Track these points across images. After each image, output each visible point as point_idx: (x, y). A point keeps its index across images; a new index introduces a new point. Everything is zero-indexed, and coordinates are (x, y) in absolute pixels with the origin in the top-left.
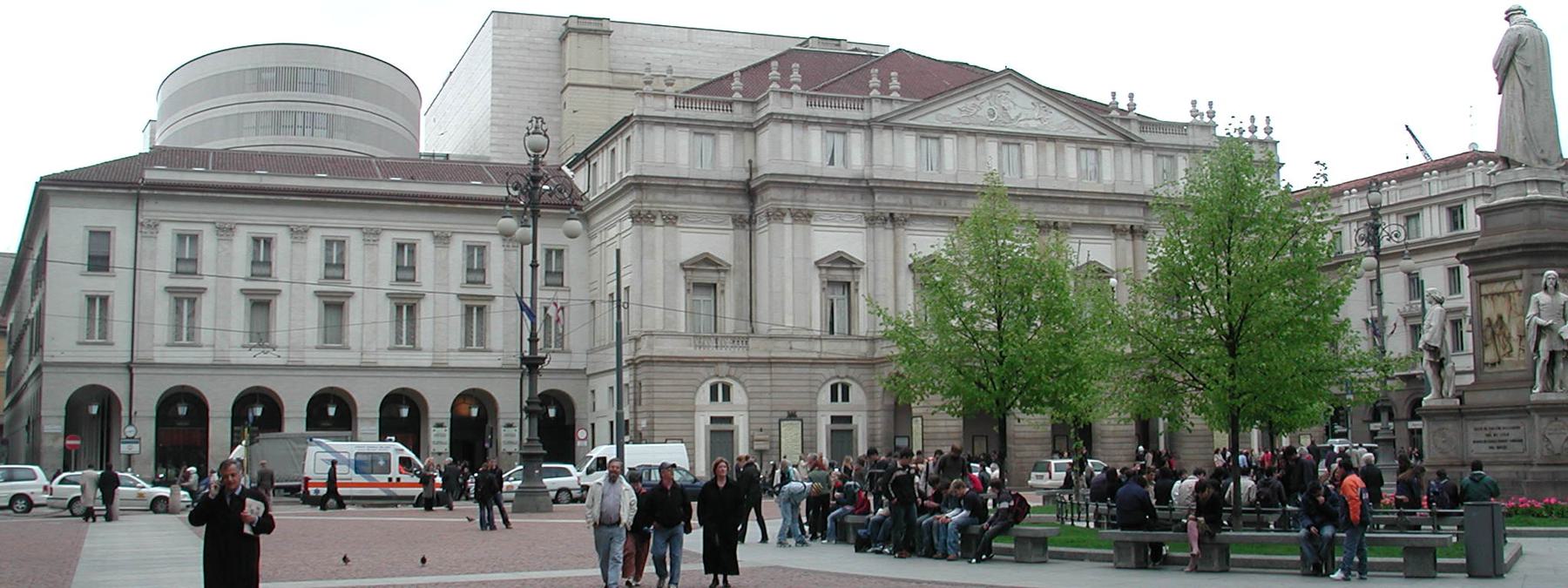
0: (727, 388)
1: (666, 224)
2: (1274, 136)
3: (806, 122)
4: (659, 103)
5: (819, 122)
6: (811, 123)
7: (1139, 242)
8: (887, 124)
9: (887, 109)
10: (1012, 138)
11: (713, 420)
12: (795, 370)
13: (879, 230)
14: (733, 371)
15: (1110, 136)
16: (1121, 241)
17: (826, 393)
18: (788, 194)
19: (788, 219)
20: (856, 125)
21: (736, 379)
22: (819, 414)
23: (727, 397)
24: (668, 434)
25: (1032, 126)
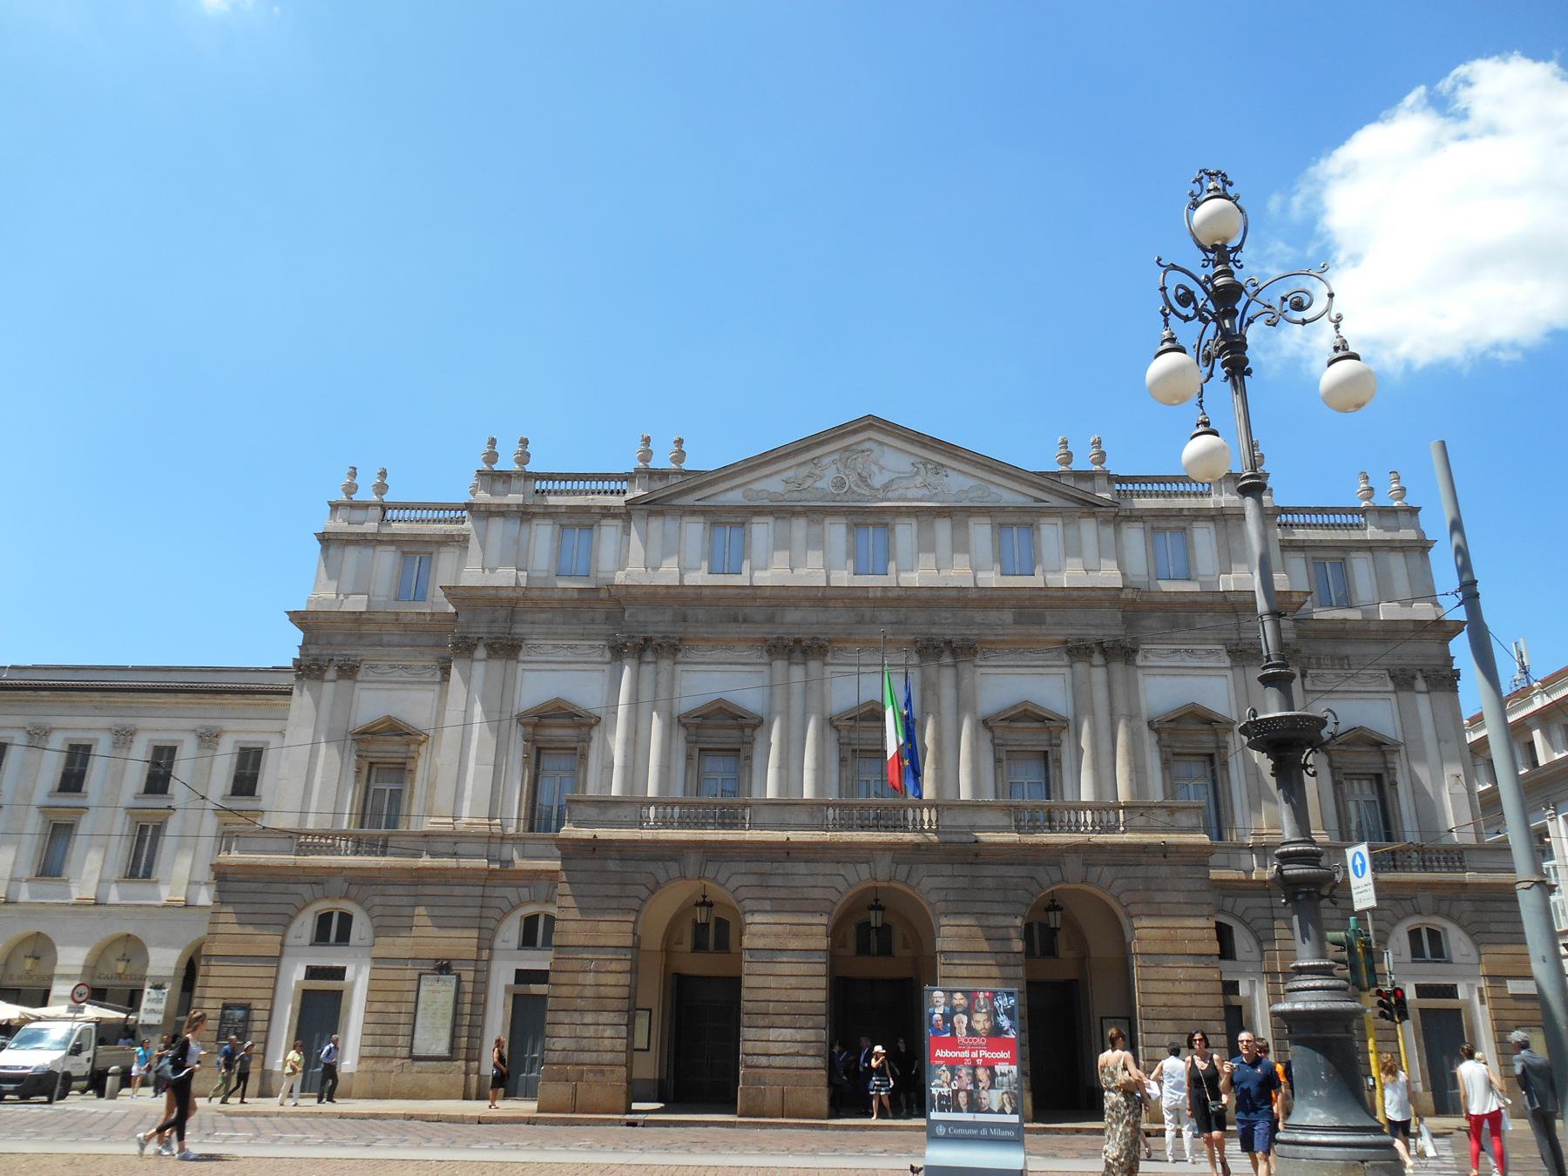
0: (346, 919)
1: (340, 677)
2: (1410, 501)
3: (525, 514)
5: (550, 513)
6: (534, 515)
7: (1118, 667)
8: (653, 507)
9: (658, 485)
10: (870, 519)
11: (313, 973)
12: (457, 890)
14: (354, 890)
15: (1055, 502)
17: (511, 931)
19: (481, 652)
20: (607, 513)
21: (360, 904)
22: (495, 965)
23: (344, 937)
24: (228, 993)
25: (915, 494)
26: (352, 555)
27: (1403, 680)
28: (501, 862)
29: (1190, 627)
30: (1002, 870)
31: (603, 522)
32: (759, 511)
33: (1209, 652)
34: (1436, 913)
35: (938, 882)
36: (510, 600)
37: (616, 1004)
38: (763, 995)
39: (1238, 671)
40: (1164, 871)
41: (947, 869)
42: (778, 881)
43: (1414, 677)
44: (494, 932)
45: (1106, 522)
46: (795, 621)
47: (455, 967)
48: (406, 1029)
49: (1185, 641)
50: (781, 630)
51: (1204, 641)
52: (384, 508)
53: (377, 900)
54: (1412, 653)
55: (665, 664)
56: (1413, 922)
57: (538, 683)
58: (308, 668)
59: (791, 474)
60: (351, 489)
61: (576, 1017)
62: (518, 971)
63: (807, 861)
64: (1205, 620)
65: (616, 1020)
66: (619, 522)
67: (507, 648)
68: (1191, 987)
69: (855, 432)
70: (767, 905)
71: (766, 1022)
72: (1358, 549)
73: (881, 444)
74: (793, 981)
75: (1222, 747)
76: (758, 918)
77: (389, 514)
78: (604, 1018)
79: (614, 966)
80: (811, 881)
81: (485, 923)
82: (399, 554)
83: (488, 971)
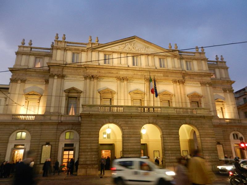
2: (224, 60)
4: (25, 49)
6: (67, 50)
7: (181, 85)
8: (93, 50)
10: (135, 56)
13: (88, 80)
14: (26, 127)
16: (175, 85)
18: (57, 70)
19: (56, 77)
22: (60, 143)
25: (143, 52)
26: (24, 57)
27: (225, 91)
28: (61, 121)
29: (193, 79)
30: (174, 121)
31: (82, 52)
32: (113, 52)
33: (197, 84)
34: (237, 131)
35: (162, 123)
37: (95, 150)
38: (127, 147)
39: (202, 87)
40: (204, 121)
41: (163, 120)
42: (130, 123)
43: (227, 90)
44: (60, 136)
46: (122, 73)
47: (51, 143)
48: (39, 158)
49: (193, 81)
50: (119, 75)
51: (196, 81)
52: (31, 48)
53: (32, 129)
54: (226, 86)
55: (95, 81)
56: (234, 132)
57: (68, 84)
58: (13, 80)
59: (119, 46)
60: (23, 44)
61: (86, 153)
62: (65, 144)
63: (135, 119)
64: (196, 78)
65: (95, 154)
66: (85, 53)
67: (62, 77)
68: (210, 144)
69: (132, 39)
70: (127, 128)
71: (129, 153)
72: (217, 68)
73: (137, 42)
74: (134, 144)
75: (200, 100)
76: (126, 131)
77: (33, 49)
78: (93, 153)
79: (94, 142)
80: (136, 123)
81: (58, 134)
82: (35, 58)
83: (58, 144)
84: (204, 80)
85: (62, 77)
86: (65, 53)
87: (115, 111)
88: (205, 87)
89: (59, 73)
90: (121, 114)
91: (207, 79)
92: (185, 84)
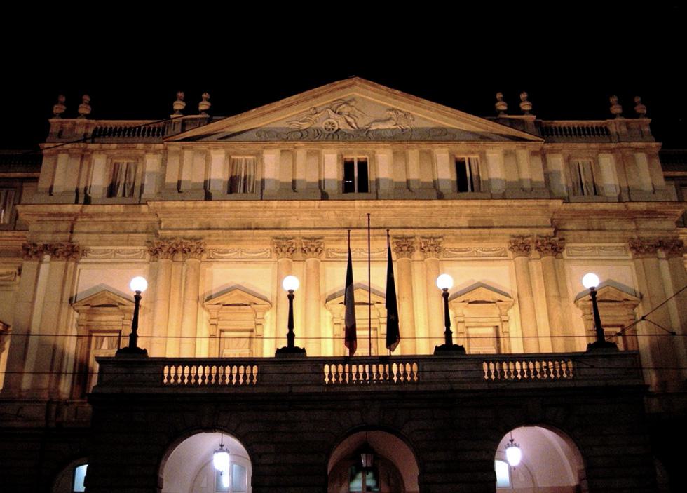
7: (549, 258)
16: (521, 259)
18: (50, 227)
36: (70, 215)
39: (639, 261)
45: (534, 153)
49: (599, 240)
51: (611, 240)
84: (647, 230)
85: (70, 252)
86: (85, 163)
87: (227, 381)
88: (651, 261)
89: (59, 238)
90: (236, 395)
91: (660, 227)
92: (564, 253)
